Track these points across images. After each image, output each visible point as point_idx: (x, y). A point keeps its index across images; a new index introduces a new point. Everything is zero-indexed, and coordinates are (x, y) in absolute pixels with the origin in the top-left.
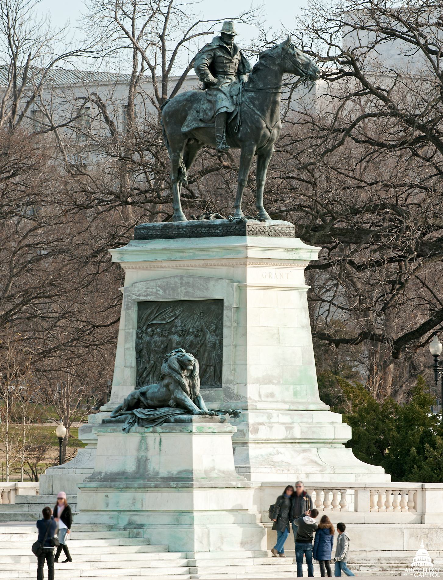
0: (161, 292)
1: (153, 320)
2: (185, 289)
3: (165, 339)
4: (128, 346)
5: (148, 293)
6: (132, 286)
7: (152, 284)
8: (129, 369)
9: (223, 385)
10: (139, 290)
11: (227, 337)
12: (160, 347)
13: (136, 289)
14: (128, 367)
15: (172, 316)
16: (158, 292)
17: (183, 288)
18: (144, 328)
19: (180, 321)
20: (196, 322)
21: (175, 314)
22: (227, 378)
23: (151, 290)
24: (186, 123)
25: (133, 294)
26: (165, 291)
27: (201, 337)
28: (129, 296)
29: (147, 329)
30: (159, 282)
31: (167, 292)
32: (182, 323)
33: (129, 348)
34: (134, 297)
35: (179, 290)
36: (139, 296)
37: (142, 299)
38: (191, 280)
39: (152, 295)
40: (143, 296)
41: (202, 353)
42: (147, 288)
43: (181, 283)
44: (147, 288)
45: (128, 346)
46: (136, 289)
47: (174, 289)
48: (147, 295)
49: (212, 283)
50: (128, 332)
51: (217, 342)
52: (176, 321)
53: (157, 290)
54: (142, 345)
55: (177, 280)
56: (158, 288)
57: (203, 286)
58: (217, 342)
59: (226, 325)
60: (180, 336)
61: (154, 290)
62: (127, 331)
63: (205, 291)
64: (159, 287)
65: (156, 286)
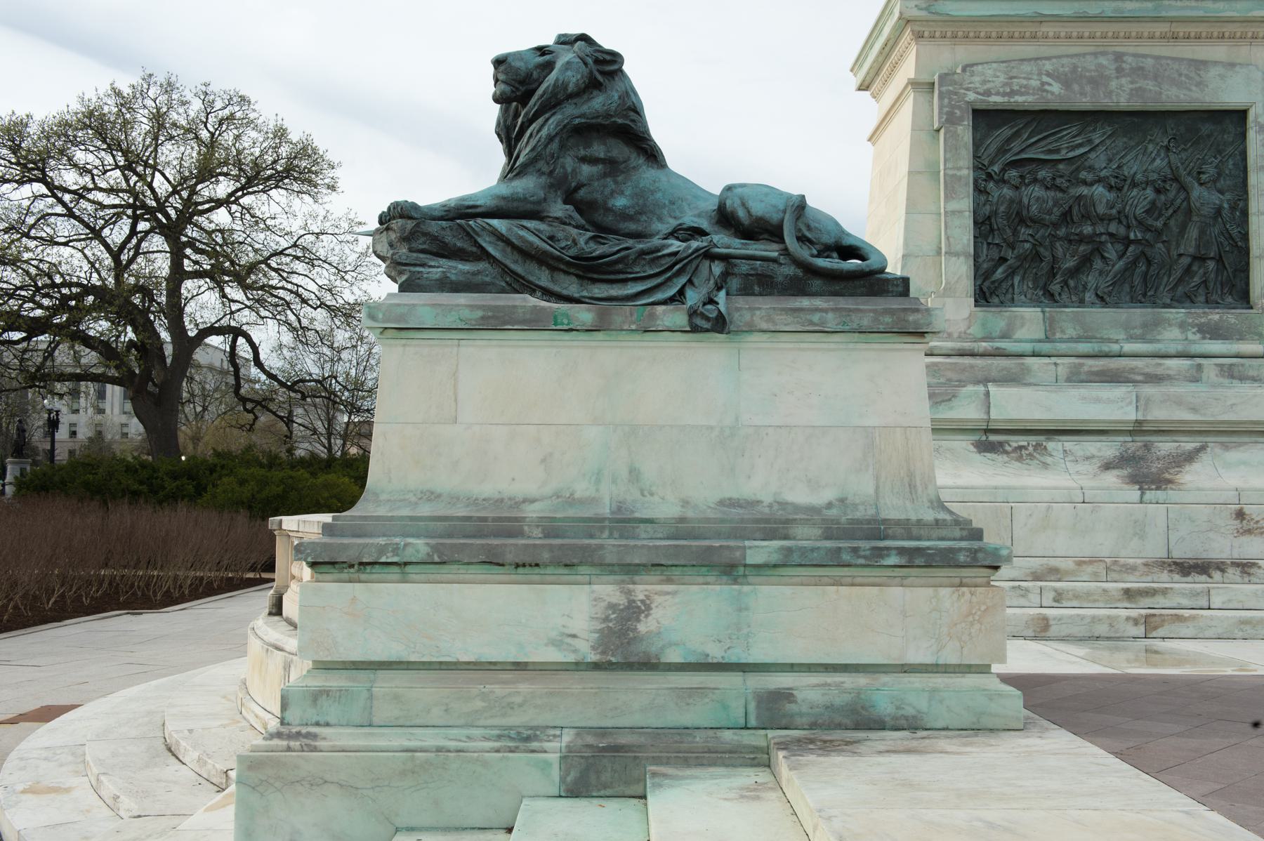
0: (1056, 88)
1: (1022, 151)
2: (1132, 83)
3: (1059, 195)
4: (954, 205)
5: (1016, 88)
8: (962, 259)
10: (984, 82)
12: (1050, 212)
13: (977, 79)
14: (957, 255)
15: (1080, 145)
16: (1047, 87)
17: (1124, 81)
19: (1103, 157)
20: (1154, 159)
21: (1090, 141)
23: (1025, 82)
25: (968, 89)
26: (1066, 84)
27: (1174, 193)
28: (956, 94)
29: (1003, 170)
31: (1076, 87)
32: (1110, 160)
33: (960, 212)
34: (971, 96)
35: (1113, 84)
36: (988, 93)
37: (996, 100)
40: (998, 94)
41: (1175, 230)
42: (1011, 78)
44: (1011, 78)
45: (954, 205)
47: (1097, 81)
48: (1013, 93)
50: (954, 176)
52: (1093, 155)
53: (1043, 84)
54: (988, 207)
56: (1045, 79)
57: (1187, 76)
60: (1110, 188)
61: (1035, 83)
62: (950, 172)
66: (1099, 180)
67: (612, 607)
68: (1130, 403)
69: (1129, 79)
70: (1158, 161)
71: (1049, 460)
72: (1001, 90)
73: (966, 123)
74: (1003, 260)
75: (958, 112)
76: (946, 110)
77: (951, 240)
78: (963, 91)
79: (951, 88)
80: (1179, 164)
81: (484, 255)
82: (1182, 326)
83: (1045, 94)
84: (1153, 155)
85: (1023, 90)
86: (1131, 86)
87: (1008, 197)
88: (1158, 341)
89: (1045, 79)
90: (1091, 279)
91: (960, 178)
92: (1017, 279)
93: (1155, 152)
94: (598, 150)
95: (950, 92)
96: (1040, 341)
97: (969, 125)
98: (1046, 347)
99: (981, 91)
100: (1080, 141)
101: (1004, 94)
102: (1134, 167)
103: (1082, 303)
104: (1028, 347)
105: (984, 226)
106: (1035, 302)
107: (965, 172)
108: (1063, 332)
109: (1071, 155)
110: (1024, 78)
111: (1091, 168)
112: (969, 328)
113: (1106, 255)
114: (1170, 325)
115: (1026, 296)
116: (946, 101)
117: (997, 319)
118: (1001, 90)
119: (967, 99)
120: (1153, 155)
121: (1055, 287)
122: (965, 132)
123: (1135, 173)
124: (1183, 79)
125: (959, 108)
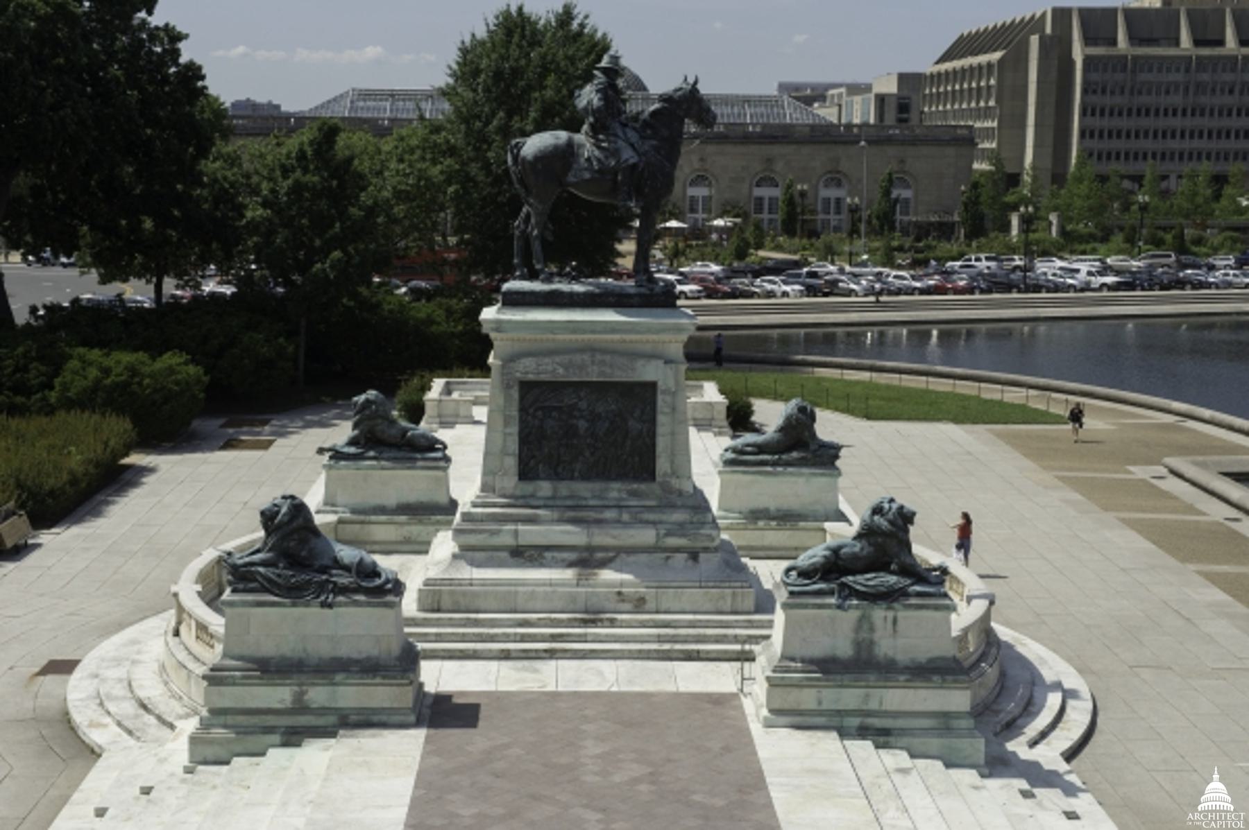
0: (561, 371)
4: (508, 430)
7: (547, 360)
9: (658, 479)
10: (525, 367)
14: (508, 455)
17: (595, 368)
26: (566, 368)
29: (536, 410)
30: (557, 359)
31: (571, 371)
34: (518, 375)
35: (589, 370)
36: (527, 373)
37: (531, 377)
43: (593, 363)
45: (508, 430)
48: (539, 373)
56: (555, 365)
60: (588, 421)
64: (557, 363)
66: (582, 417)
67: (296, 692)
71: (544, 561)
74: (533, 457)
81: (256, 580)
82: (619, 491)
88: (607, 499)
90: (578, 466)
94: (296, 536)
96: (548, 498)
98: (550, 503)
102: (600, 408)
103: (572, 478)
104: (541, 503)
105: (524, 440)
111: (579, 410)
117: (528, 487)
121: (560, 470)
122: (515, 393)
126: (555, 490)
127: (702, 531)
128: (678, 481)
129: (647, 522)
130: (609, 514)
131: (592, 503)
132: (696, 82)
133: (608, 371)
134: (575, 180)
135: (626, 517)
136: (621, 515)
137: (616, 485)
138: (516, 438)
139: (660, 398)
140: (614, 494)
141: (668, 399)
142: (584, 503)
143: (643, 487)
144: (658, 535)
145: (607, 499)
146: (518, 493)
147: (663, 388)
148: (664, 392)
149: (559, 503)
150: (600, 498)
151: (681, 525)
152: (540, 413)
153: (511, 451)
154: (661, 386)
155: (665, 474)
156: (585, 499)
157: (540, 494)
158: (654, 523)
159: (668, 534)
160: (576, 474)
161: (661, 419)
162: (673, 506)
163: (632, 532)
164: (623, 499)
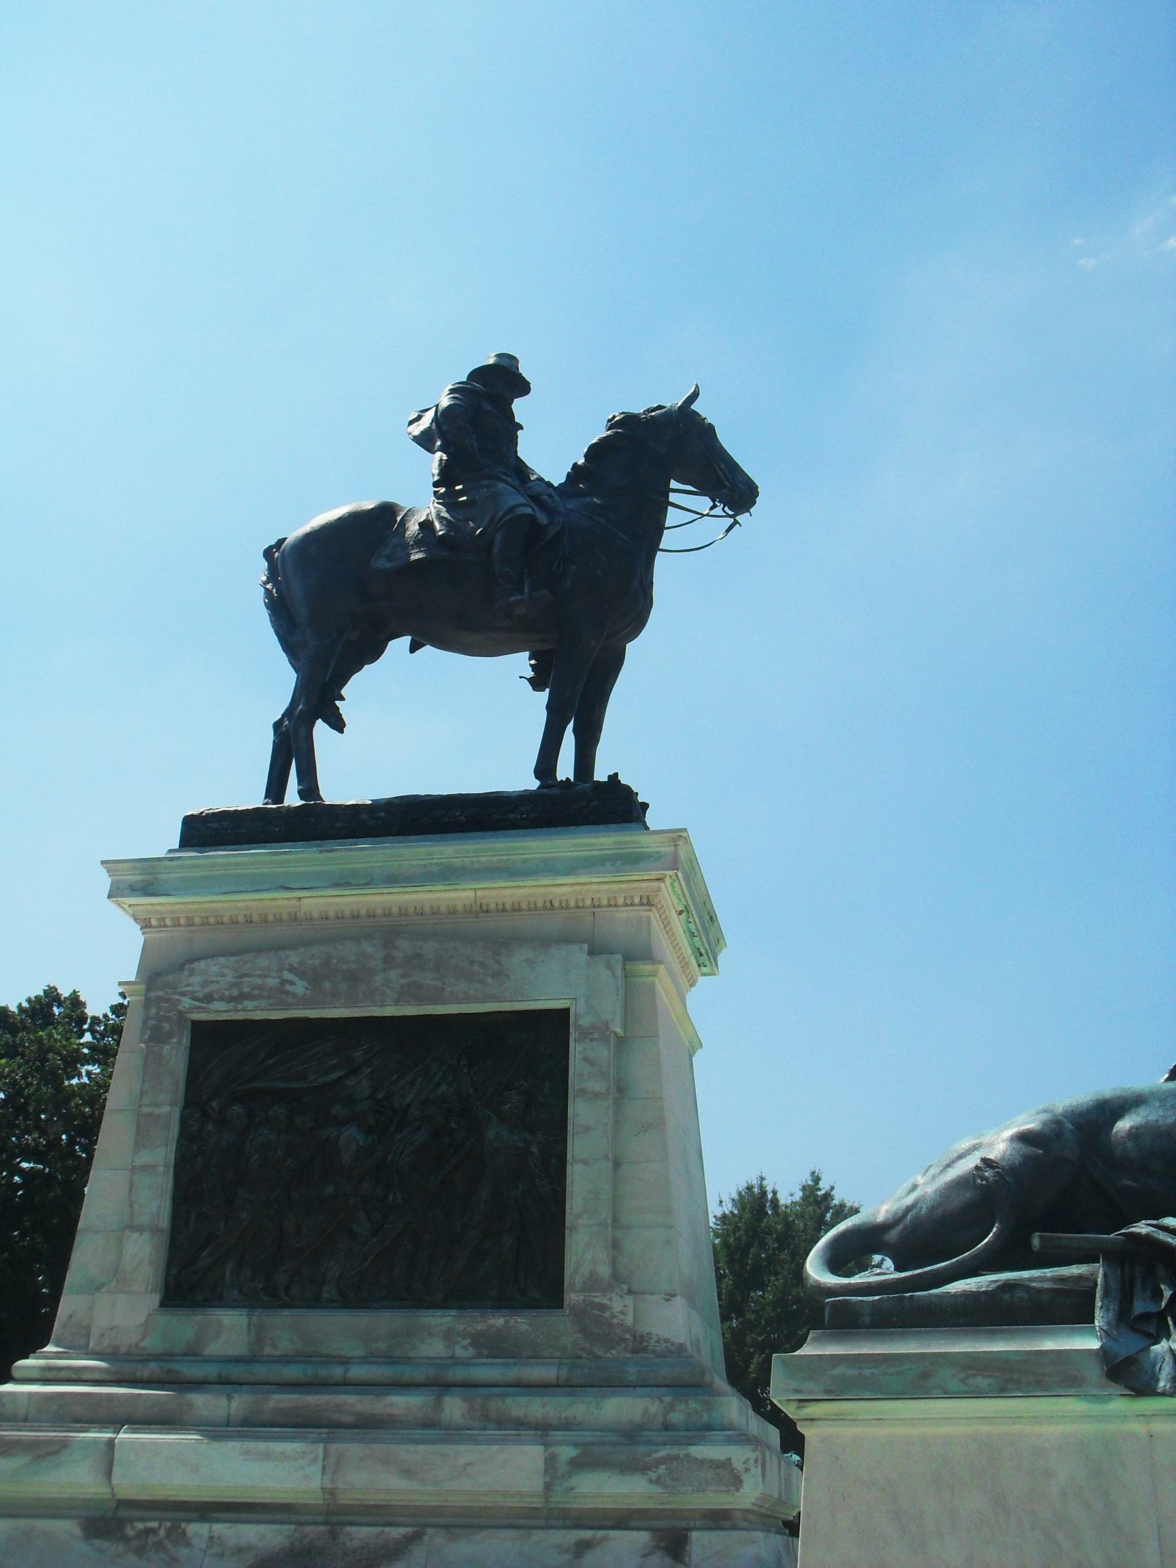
0: (300, 987)
2: (403, 976)
4: (144, 1158)
5: (246, 990)
6: (182, 968)
7: (263, 961)
8: (146, 1235)
9: (572, 1297)
10: (205, 983)
11: (587, 1129)
13: (196, 979)
14: (140, 1229)
16: (288, 987)
17: (392, 974)
18: (214, 1104)
20: (438, 1085)
22: (592, 1273)
23: (259, 981)
24: (387, 552)
25: (183, 994)
28: (167, 1000)
30: (293, 958)
31: (327, 985)
35: (379, 979)
36: (209, 998)
37: (220, 1011)
38: (429, 948)
39: (261, 997)
43: (388, 959)
45: (144, 1158)
46: (196, 979)
48: (242, 997)
49: (517, 958)
50: (149, 1115)
51: (534, 1150)
52: (350, 1082)
53: (284, 982)
54: (199, 1160)
55: (368, 948)
56: (287, 975)
58: (534, 1150)
59: (583, 1091)
62: (146, 1110)
63: (490, 980)
64: (292, 970)
65: (281, 970)
68: (315, 1460)
69: (400, 971)
70: (444, 1087)
72: (227, 993)
73: (175, 1040)
75: (166, 1026)
76: (151, 1023)
77: (136, 1207)
78: (176, 997)
79: (161, 993)
80: (471, 1091)
82: (448, 1336)
83: (284, 997)
84: (437, 1078)
85: (256, 992)
86: (403, 981)
87: (224, 1143)
89: (287, 975)
91: (158, 1118)
92: (229, 1267)
93: (440, 1074)
95: (160, 999)
96: (237, 1360)
97: (180, 1043)
98: (237, 1372)
99: (200, 995)
100: (335, 1061)
101: (231, 999)
103: (315, 1302)
104: (210, 1371)
106: (249, 1301)
107: (166, 1109)
108: (274, 1346)
109: (321, 1080)
110: (260, 976)
112: (143, 1339)
113: (355, 1227)
114: (430, 1334)
115: (241, 1291)
116: (153, 1011)
118: (227, 993)
119: (180, 1007)
120: (437, 1078)
123: (409, 1106)
124: (476, 968)
125: (168, 1019)
126: (259, 1335)
127: (700, 1451)
128: (629, 1301)
129: (521, 1424)
130: (400, 1403)
131: (358, 1372)
132: (695, 396)
133: (428, 979)
134: (388, 565)
135: (454, 1407)
136: (438, 1405)
137: (440, 1320)
138: (168, 1183)
139: (576, 1050)
140: (434, 1348)
141: (602, 1052)
142: (337, 1372)
143: (521, 1323)
144: (550, 1462)
145: (407, 1360)
146: (152, 1343)
147: (584, 1022)
148: (584, 1034)
149: (261, 1371)
150: (390, 1359)
151: (631, 1434)
152: (237, 1109)
153: (143, 1219)
154: (581, 1019)
155: (592, 1283)
156: (346, 1361)
157: (215, 1348)
158: (543, 1430)
159: (583, 1463)
160: (327, 1292)
161: (579, 1111)
162: (614, 1383)
163: (465, 1453)
164: (455, 1361)
